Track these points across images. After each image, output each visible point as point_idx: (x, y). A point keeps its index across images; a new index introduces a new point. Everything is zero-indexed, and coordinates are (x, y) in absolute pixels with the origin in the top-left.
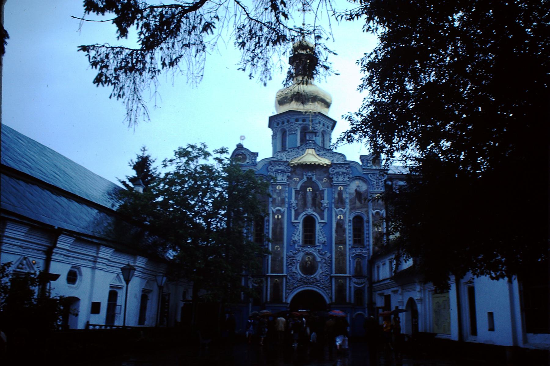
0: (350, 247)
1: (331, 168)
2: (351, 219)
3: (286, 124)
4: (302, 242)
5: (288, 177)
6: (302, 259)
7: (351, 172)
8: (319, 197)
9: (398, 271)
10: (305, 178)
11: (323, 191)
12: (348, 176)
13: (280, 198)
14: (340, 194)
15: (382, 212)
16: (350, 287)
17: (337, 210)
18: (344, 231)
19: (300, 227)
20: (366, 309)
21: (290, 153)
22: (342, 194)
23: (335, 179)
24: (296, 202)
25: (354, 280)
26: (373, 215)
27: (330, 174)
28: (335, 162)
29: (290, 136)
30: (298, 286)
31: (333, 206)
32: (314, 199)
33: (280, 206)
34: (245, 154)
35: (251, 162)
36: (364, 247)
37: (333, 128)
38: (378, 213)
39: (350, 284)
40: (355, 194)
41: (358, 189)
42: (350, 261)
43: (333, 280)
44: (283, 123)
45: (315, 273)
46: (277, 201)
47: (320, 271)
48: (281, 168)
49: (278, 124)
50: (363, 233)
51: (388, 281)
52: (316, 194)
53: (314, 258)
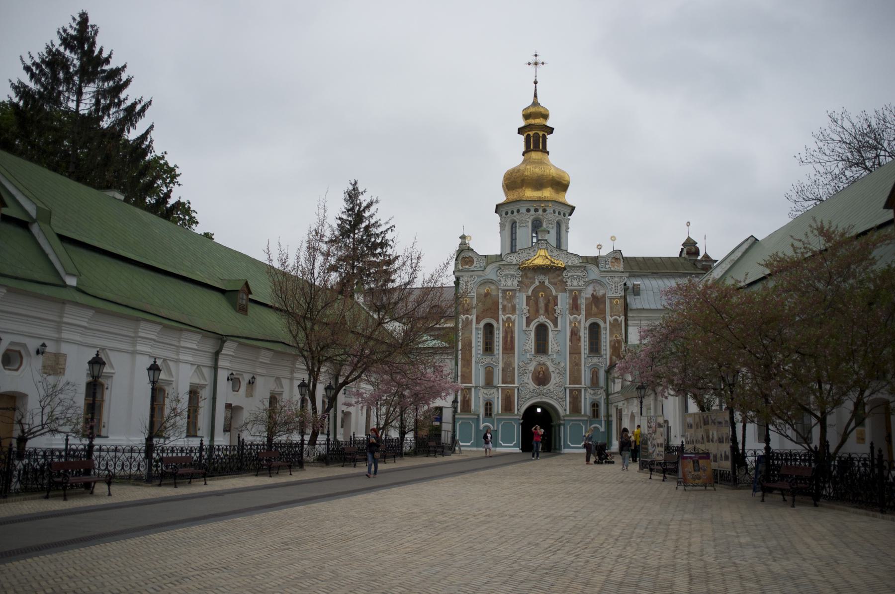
2: (587, 325)
3: (515, 213)
10: (537, 283)
11: (557, 297)
14: (575, 299)
15: (620, 319)
17: (572, 317)
18: (579, 340)
19: (533, 335)
23: (569, 283)
25: (590, 391)
28: (570, 264)
32: (546, 306)
37: (570, 215)
38: (616, 320)
44: (512, 212)
49: (507, 213)
53: (547, 369)
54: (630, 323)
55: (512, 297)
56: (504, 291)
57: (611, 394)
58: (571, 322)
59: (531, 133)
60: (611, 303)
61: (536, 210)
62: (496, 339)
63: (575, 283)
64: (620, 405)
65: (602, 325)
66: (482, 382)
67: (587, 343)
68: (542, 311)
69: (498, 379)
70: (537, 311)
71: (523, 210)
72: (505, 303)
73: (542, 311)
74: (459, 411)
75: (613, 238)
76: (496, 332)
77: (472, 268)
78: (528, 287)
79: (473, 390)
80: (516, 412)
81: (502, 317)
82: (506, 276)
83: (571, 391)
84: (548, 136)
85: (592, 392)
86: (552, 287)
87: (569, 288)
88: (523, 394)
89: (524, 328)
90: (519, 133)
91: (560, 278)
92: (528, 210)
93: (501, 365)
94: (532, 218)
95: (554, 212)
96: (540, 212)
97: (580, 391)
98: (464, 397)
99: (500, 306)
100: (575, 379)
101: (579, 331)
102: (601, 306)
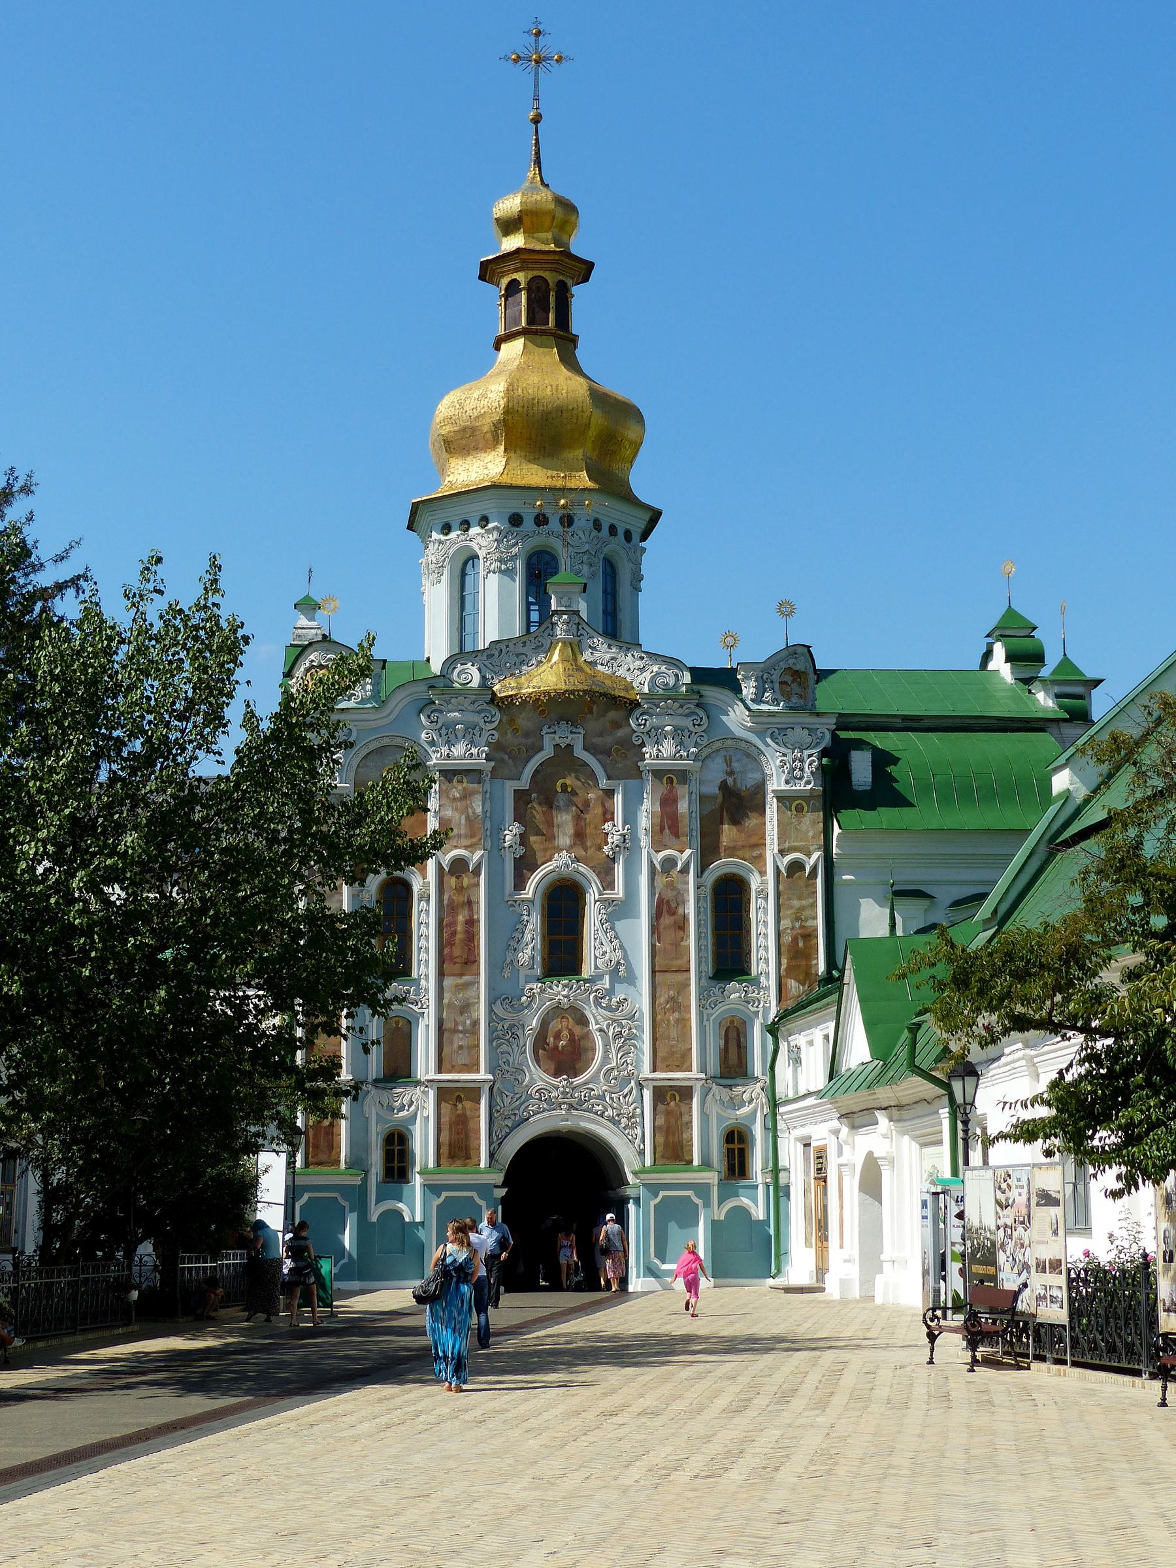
1: (637, 713)
4: (544, 966)
8: (598, 811)
13: (463, 817)
18: (682, 926)
20: (761, 1190)
21: (495, 660)
31: (644, 841)
33: (466, 847)
37: (645, 536)
38: (796, 867)
40: (720, 800)
41: (730, 781)
43: (647, 1094)
51: (811, 1101)
59: (520, 277)
61: (541, 520)
65: (755, 882)
68: (564, 840)
69: (424, 1063)
72: (448, 813)
73: (564, 840)
75: (786, 609)
84: (575, 290)
90: (482, 277)
91: (620, 733)
92: (516, 520)
96: (554, 524)
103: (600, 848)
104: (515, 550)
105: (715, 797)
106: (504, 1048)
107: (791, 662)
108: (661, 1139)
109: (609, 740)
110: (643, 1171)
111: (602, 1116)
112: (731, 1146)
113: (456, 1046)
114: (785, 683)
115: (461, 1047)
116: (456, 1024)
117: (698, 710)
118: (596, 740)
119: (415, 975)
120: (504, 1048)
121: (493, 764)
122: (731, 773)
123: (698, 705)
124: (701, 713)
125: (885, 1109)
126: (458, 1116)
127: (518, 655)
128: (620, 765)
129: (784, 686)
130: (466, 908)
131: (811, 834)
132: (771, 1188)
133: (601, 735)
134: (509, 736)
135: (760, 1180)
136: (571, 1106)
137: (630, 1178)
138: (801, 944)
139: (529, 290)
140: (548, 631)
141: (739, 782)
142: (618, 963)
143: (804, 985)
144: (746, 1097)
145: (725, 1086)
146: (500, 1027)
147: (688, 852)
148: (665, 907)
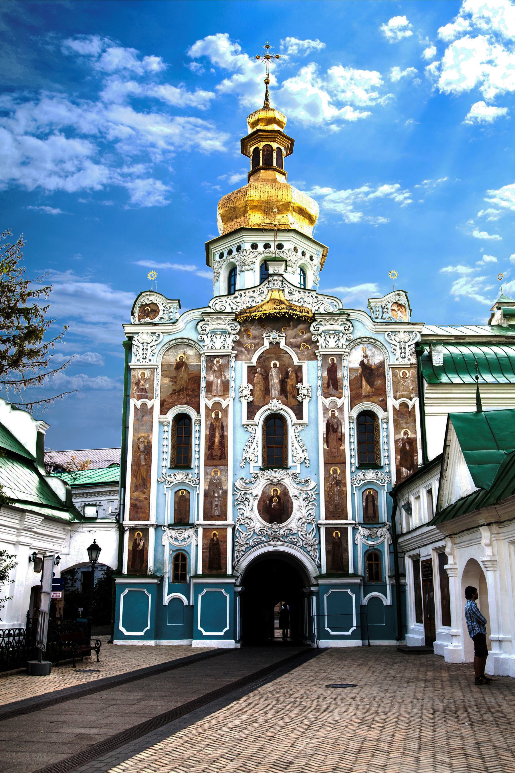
0: (353, 469)
1: (314, 324)
3: (235, 253)
5: (234, 342)
6: (263, 493)
7: (351, 328)
9: (445, 505)
10: (267, 345)
11: (301, 367)
12: (345, 337)
13: (219, 381)
14: (332, 370)
15: (410, 404)
16: (355, 545)
17: (327, 401)
18: (341, 439)
20: (388, 587)
21: (237, 300)
22: (336, 372)
24: (251, 387)
25: (362, 530)
26: (394, 408)
27: (313, 335)
28: (322, 311)
29: (242, 274)
30: (257, 544)
31: (320, 392)
32: (283, 383)
34: (156, 304)
35: (166, 317)
36: (382, 468)
38: (404, 405)
39: (354, 540)
40: (360, 371)
41: (366, 361)
42: (353, 494)
44: (230, 252)
45: (288, 517)
46: (214, 388)
47: (296, 514)
48: (220, 326)
49: (221, 256)
50: (378, 442)
52: (287, 373)
53: (285, 492)
54: (427, 410)
55: (222, 369)
56: (210, 358)
57: (403, 535)
58: (326, 410)
60: (394, 375)
61: (267, 246)
62: (194, 441)
63: (332, 343)
64: (428, 552)
66: (169, 517)
67: (355, 446)
68: (275, 393)
70: (267, 391)
71: (247, 246)
72: (211, 378)
73: (275, 393)
74: (125, 571)
76: (195, 428)
77: (156, 320)
78: (251, 351)
79: (152, 531)
80: (229, 572)
81: (205, 402)
82: (214, 333)
83: (329, 531)
85: (367, 532)
86: (291, 352)
87: (322, 351)
88: (242, 538)
89: (245, 421)
91: (305, 336)
92: (254, 246)
93: (203, 486)
94: (260, 257)
95: (295, 249)
97: (344, 531)
98: (135, 545)
99: (203, 384)
100: (336, 508)
101: (340, 424)
102: (378, 383)
103: (294, 397)
104: (254, 260)
105: (357, 369)
106: (241, 507)
107: (397, 298)
108: (330, 558)
109: (299, 340)
110: (321, 576)
111: (295, 545)
112: (370, 562)
113: (214, 505)
114: (394, 310)
115: (216, 506)
116: (214, 493)
117: (347, 322)
118: (292, 340)
119: (193, 466)
120: (241, 507)
121: (236, 352)
122: (366, 357)
123: (347, 320)
124: (349, 324)
125: (488, 525)
126: (214, 545)
127: (250, 297)
128: (306, 353)
129: (394, 312)
130: (220, 428)
131: (411, 387)
132: (395, 587)
133: (295, 338)
134: (245, 338)
135: (388, 582)
136: (278, 539)
137: (314, 582)
138: (407, 448)
139: (263, 150)
140: (267, 285)
141: (370, 361)
142: (305, 459)
143: (410, 471)
144: (379, 534)
145: (366, 528)
146: (239, 495)
147: (343, 398)
148: (331, 428)
